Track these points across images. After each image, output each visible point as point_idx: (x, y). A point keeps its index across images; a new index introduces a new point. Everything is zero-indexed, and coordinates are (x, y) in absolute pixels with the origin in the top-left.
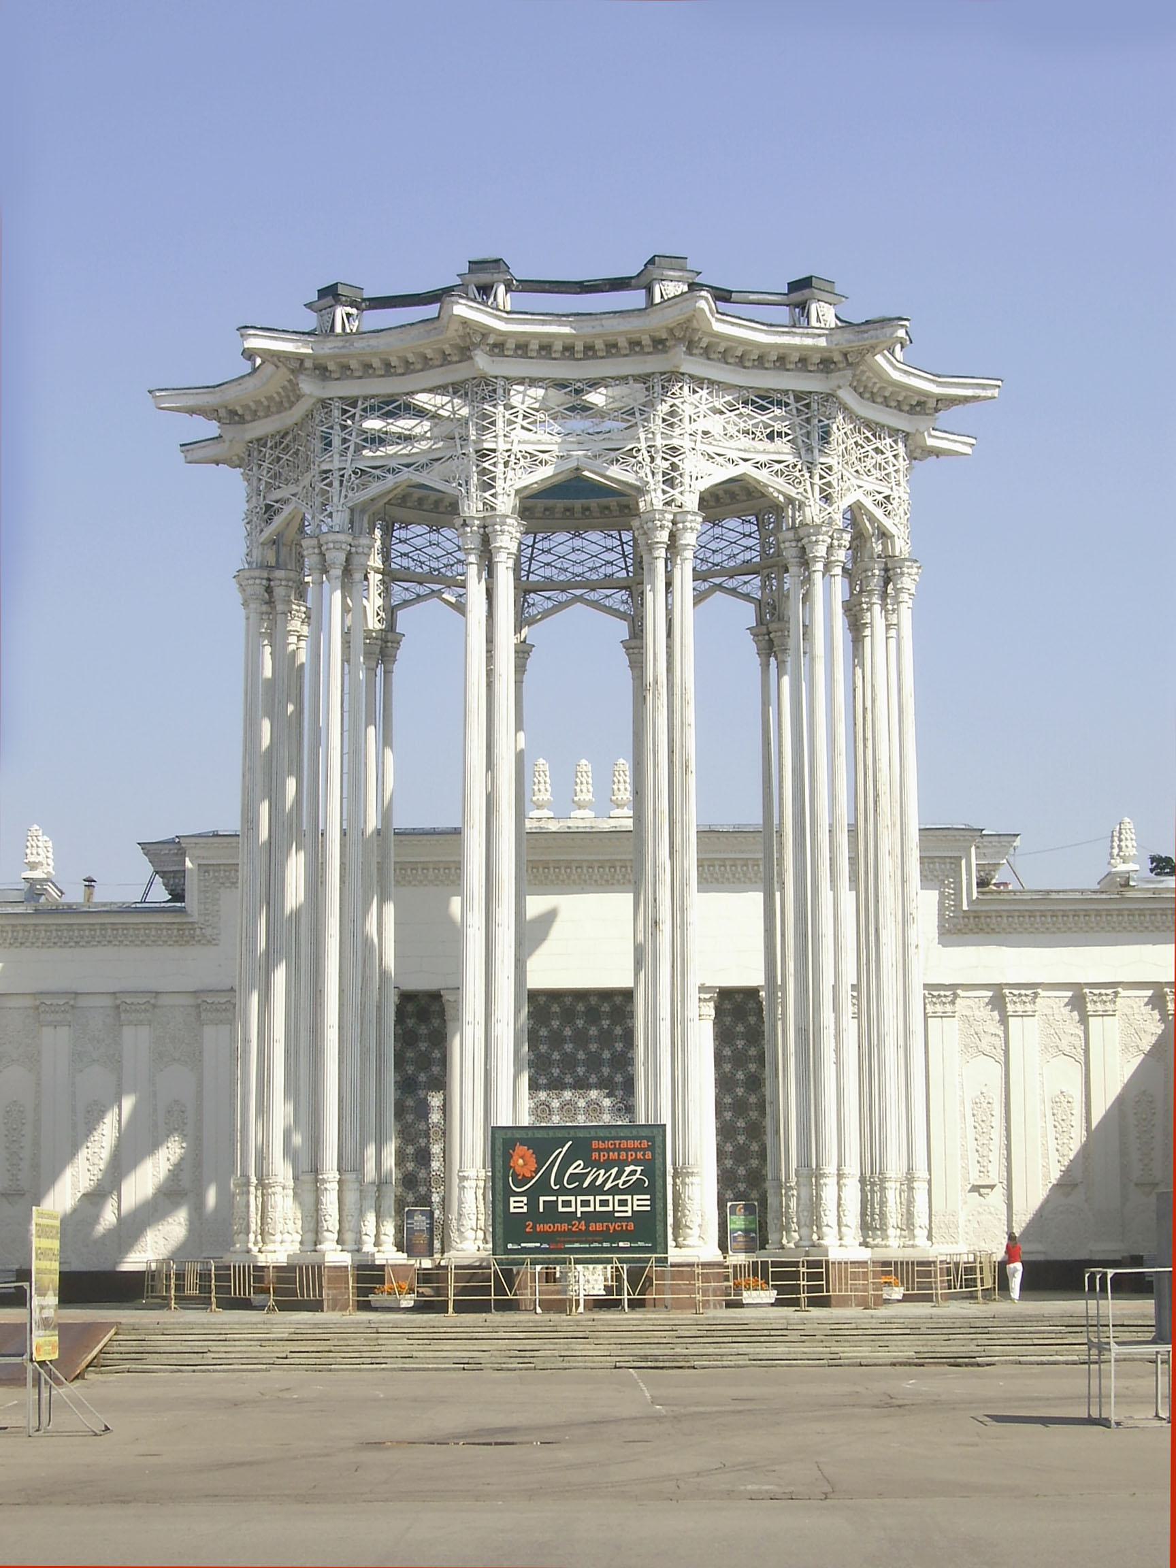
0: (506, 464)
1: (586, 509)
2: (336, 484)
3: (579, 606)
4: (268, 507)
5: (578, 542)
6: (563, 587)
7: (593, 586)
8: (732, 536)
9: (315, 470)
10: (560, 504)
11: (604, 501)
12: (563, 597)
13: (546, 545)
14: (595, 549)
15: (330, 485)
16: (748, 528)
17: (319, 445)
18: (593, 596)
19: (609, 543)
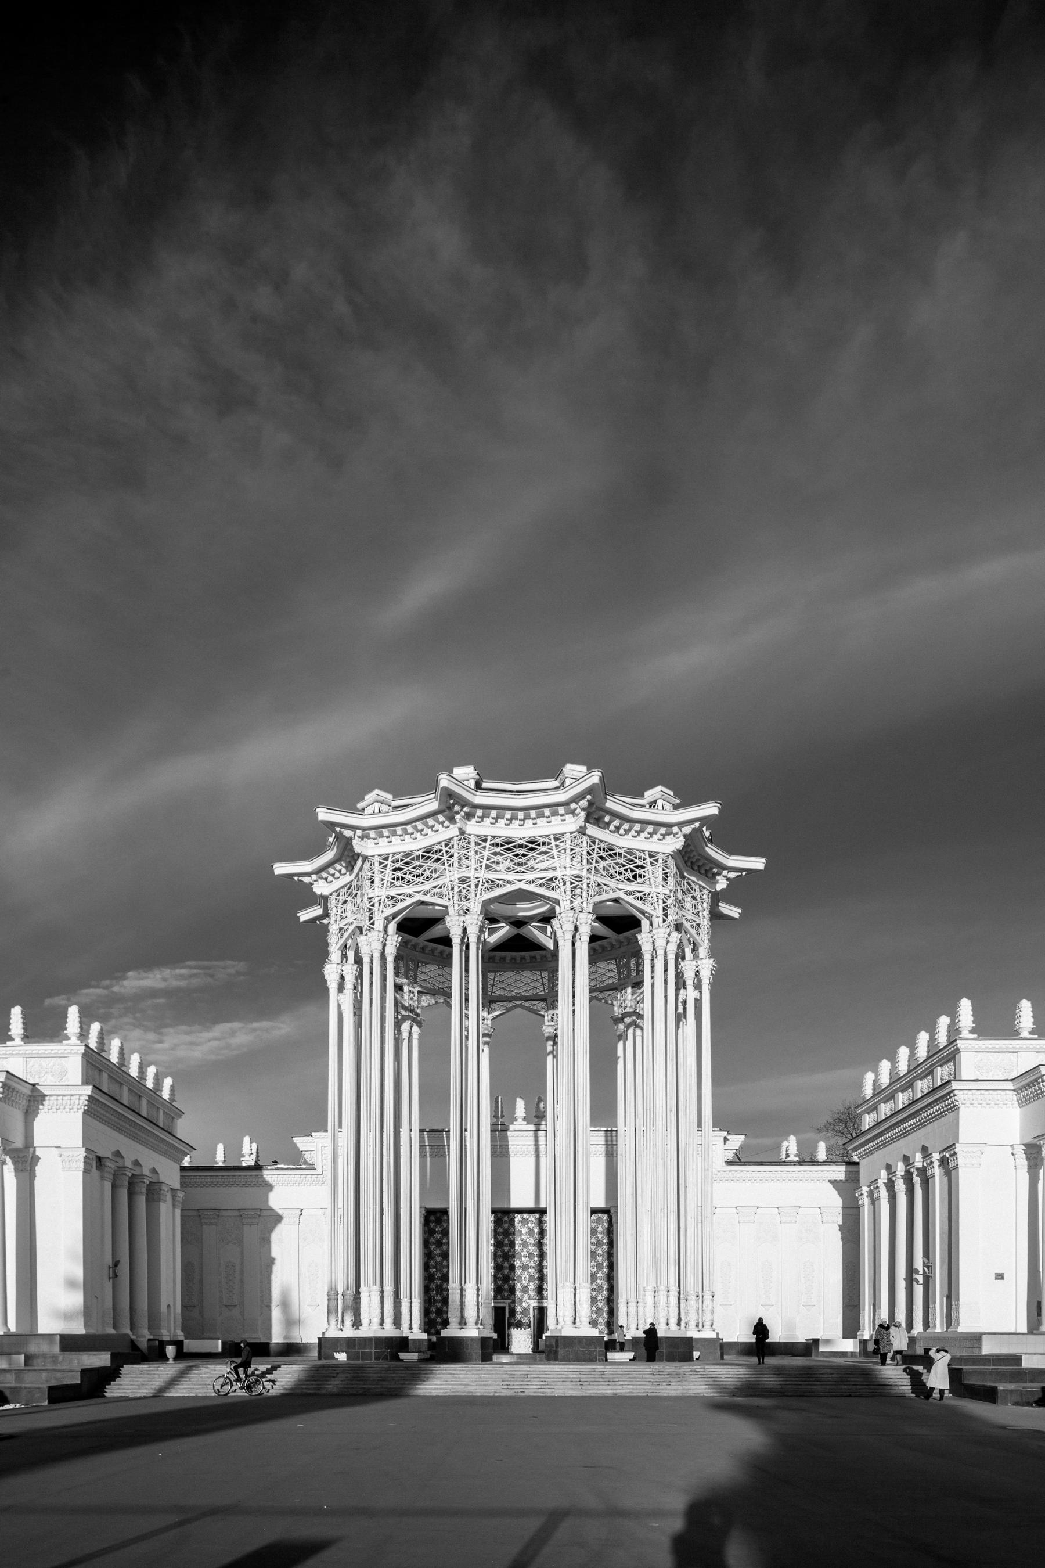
0: (477, 886)
1: (523, 958)
2: (377, 905)
3: (518, 1010)
4: (341, 929)
5: (518, 977)
6: (510, 1000)
7: (527, 999)
8: (602, 971)
9: (365, 898)
10: (509, 955)
11: (532, 953)
12: (510, 1005)
13: (501, 979)
14: (528, 981)
15: (373, 905)
16: (611, 967)
17: (368, 883)
18: (527, 1004)
19: (535, 978)
